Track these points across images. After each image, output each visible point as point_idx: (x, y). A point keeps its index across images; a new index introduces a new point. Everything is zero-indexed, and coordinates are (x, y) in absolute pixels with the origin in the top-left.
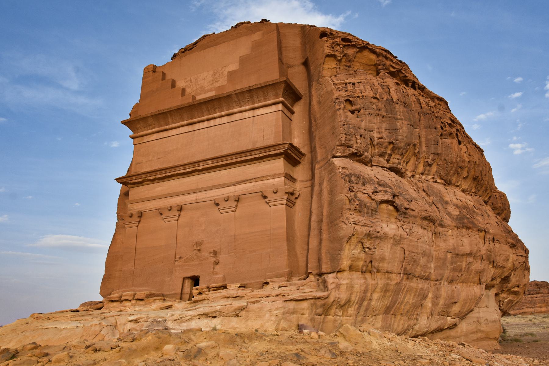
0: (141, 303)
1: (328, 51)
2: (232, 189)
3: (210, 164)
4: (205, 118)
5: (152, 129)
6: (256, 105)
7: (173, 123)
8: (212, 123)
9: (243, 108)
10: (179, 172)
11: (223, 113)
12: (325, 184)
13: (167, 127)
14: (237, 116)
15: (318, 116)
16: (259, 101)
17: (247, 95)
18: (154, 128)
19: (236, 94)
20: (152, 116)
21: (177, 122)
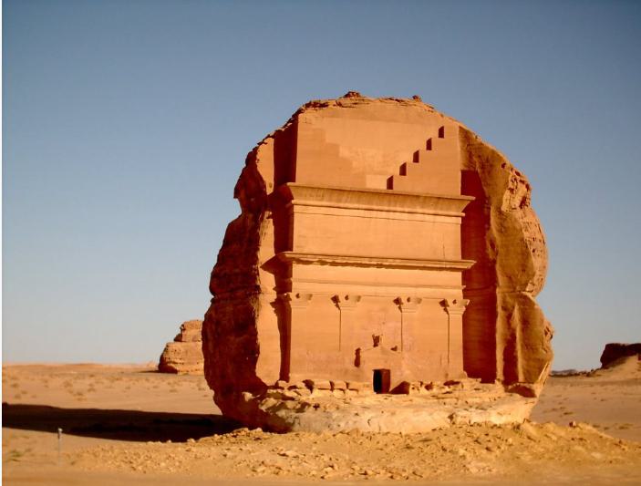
0: (355, 392)
1: (511, 185)
2: (413, 290)
3: (398, 263)
4: (386, 208)
5: (320, 200)
6: (440, 212)
7: (346, 202)
8: (391, 215)
9: (426, 211)
10: (364, 262)
11: (407, 210)
12: (516, 314)
13: (341, 205)
14: (419, 217)
15: (498, 241)
16: (441, 209)
17: (436, 200)
18: (322, 200)
19: (426, 197)
20: (328, 189)
21: (350, 202)
